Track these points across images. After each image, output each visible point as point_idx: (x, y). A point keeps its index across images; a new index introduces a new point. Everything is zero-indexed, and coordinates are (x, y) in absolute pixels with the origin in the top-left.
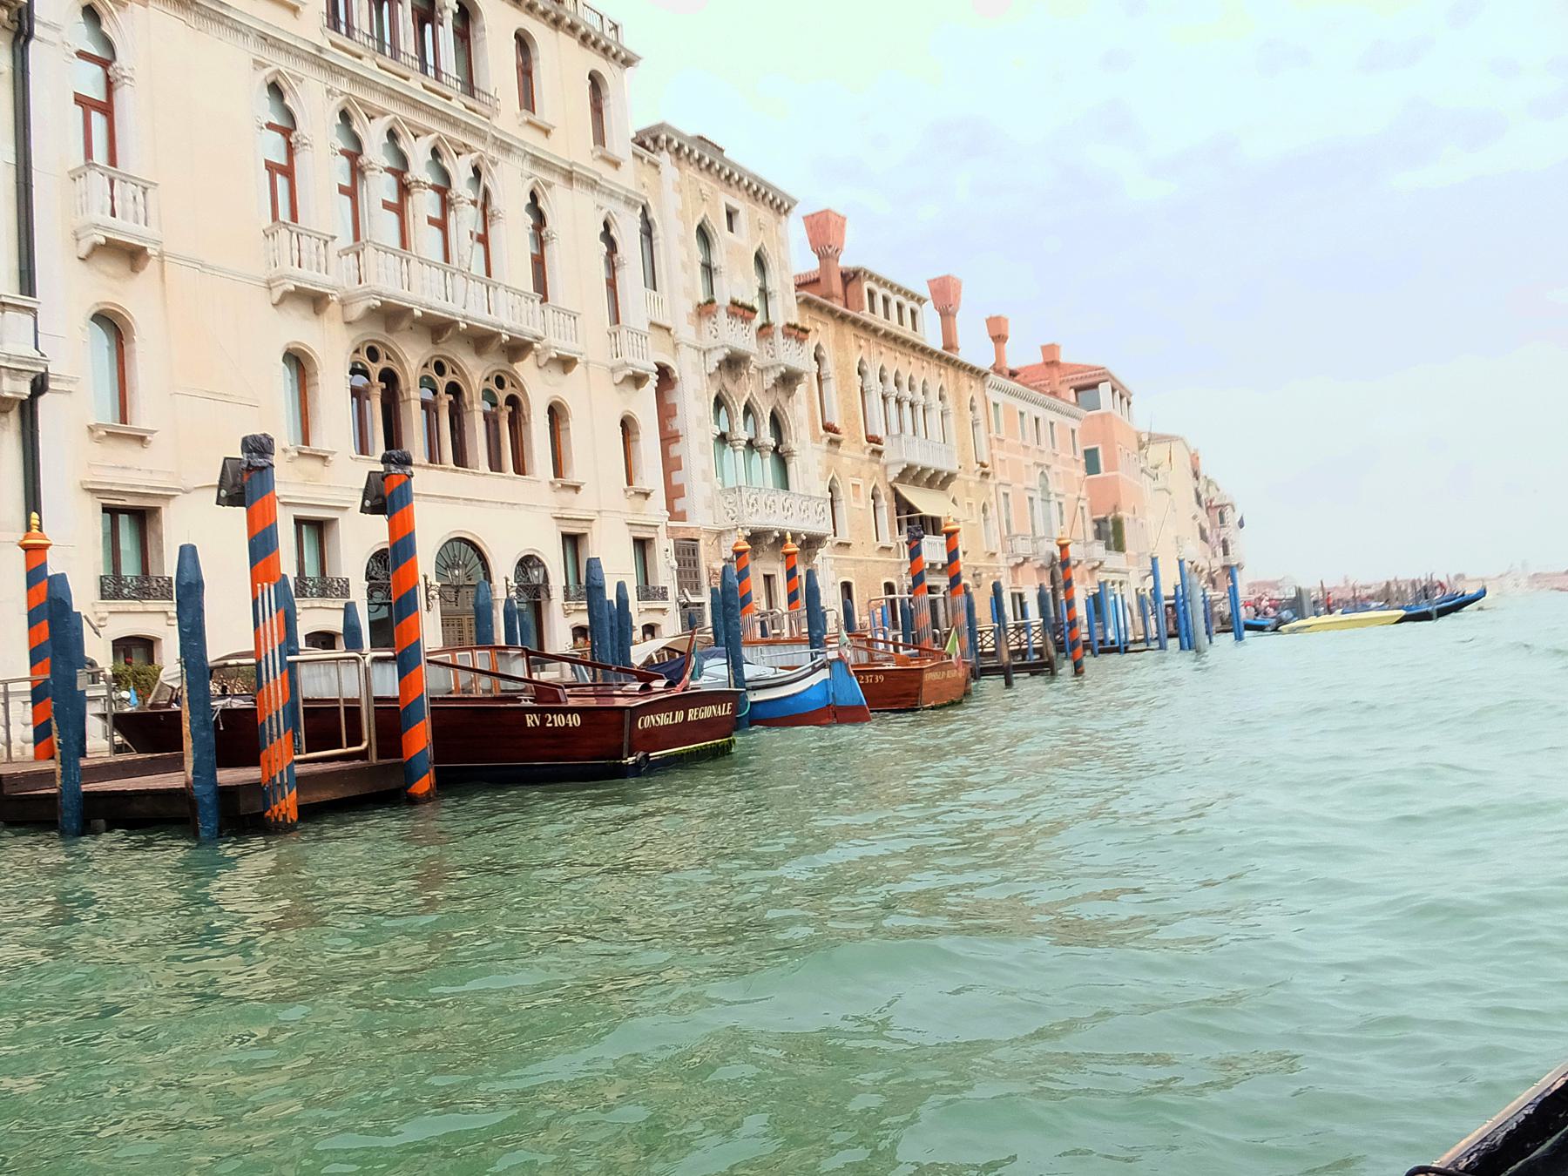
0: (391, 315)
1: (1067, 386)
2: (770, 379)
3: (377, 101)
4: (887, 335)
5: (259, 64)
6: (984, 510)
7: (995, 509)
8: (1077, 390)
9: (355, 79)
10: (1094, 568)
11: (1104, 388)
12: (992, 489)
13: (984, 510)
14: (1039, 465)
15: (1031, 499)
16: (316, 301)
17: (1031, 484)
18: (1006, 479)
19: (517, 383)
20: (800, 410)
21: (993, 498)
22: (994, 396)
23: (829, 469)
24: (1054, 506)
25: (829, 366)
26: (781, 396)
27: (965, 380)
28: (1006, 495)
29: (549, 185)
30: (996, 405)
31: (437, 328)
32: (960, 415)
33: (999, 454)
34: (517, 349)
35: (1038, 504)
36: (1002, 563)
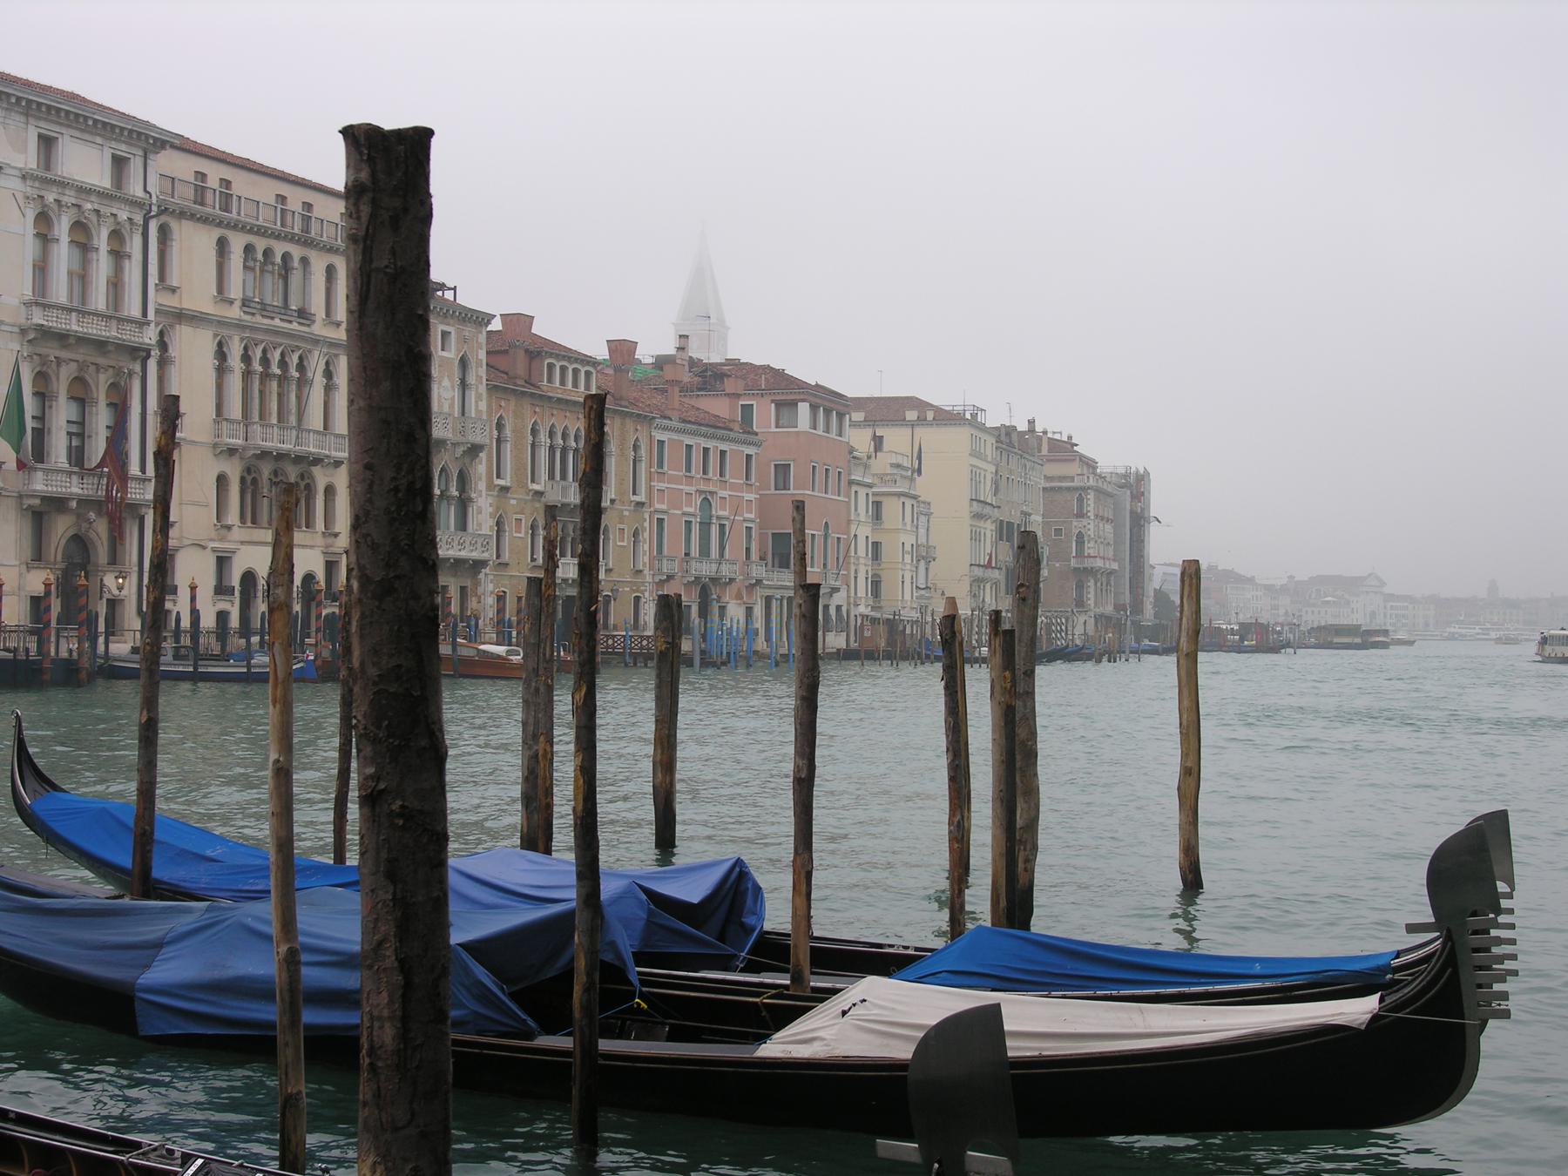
0: (264, 454)
1: (767, 399)
2: (460, 451)
3: (260, 337)
4: (559, 400)
5: (216, 335)
6: (636, 534)
7: (646, 535)
8: (779, 405)
9: (253, 329)
10: (752, 586)
11: (804, 409)
12: (647, 516)
13: (636, 534)
14: (701, 492)
15: (688, 523)
16: (232, 451)
17: (691, 510)
18: (664, 507)
19: (312, 478)
20: (481, 467)
21: (647, 524)
22: (658, 435)
23: (498, 509)
24: (714, 530)
25: (508, 432)
26: (467, 460)
27: (630, 424)
28: (660, 521)
29: (336, 356)
30: (661, 443)
31: (281, 456)
32: (622, 454)
33: (658, 485)
34: (317, 461)
35: (695, 529)
36: (649, 579)
